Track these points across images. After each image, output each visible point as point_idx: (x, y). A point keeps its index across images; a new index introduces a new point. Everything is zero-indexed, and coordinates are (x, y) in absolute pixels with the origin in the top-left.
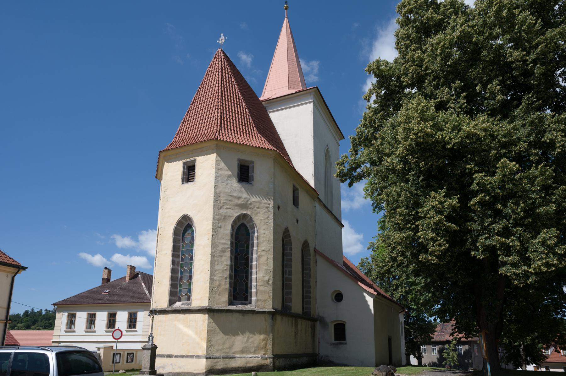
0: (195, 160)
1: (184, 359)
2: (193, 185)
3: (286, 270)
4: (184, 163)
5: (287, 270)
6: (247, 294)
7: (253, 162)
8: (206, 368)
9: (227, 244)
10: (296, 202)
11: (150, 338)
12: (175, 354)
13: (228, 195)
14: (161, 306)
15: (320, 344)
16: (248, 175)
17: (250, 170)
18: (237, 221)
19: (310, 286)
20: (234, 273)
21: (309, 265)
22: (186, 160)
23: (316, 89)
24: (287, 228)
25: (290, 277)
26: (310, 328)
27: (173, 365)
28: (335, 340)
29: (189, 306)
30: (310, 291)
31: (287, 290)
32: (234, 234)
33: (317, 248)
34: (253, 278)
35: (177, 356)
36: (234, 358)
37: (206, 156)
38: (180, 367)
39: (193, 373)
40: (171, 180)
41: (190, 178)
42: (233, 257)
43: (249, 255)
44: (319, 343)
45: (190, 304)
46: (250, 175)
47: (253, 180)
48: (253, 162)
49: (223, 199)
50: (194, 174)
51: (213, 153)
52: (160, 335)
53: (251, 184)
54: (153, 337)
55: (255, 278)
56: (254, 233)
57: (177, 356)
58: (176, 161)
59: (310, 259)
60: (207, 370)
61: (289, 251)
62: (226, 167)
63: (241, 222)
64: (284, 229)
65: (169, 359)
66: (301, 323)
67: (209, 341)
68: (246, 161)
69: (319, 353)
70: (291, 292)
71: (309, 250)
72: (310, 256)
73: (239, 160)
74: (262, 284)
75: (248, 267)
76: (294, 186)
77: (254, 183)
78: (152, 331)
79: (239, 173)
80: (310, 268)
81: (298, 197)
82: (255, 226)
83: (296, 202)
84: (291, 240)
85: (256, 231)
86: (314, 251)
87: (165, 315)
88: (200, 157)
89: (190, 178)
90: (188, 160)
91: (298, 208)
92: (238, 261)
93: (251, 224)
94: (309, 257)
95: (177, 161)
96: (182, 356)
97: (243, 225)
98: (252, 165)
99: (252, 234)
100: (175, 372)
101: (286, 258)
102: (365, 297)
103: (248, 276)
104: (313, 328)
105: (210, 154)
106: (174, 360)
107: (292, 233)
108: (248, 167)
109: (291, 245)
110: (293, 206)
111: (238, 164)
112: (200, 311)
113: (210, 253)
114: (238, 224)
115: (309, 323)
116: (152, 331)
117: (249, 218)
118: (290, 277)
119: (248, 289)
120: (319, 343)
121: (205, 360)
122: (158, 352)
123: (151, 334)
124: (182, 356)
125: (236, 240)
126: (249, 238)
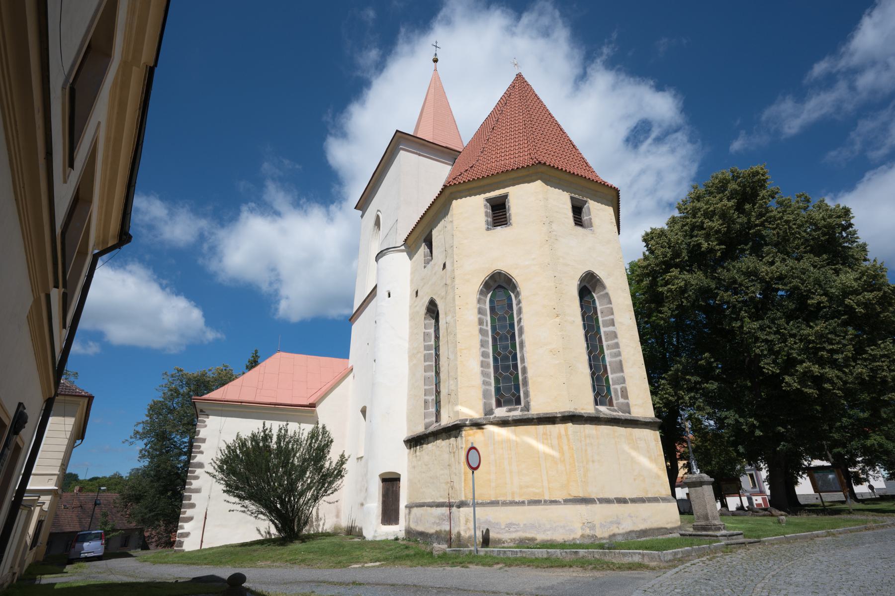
0: (586, 202)
1: (647, 505)
14: (583, 409)
27: (631, 517)
29: (526, 413)
35: (634, 501)
37: (600, 204)
38: (644, 520)
39: (666, 528)
40: (557, 212)
52: (593, 461)
57: (634, 501)
65: (604, 505)
87: (594, 426)
96: (642, 500)
100: (638, 529)
106: (630, 507)
124: (642, 500)
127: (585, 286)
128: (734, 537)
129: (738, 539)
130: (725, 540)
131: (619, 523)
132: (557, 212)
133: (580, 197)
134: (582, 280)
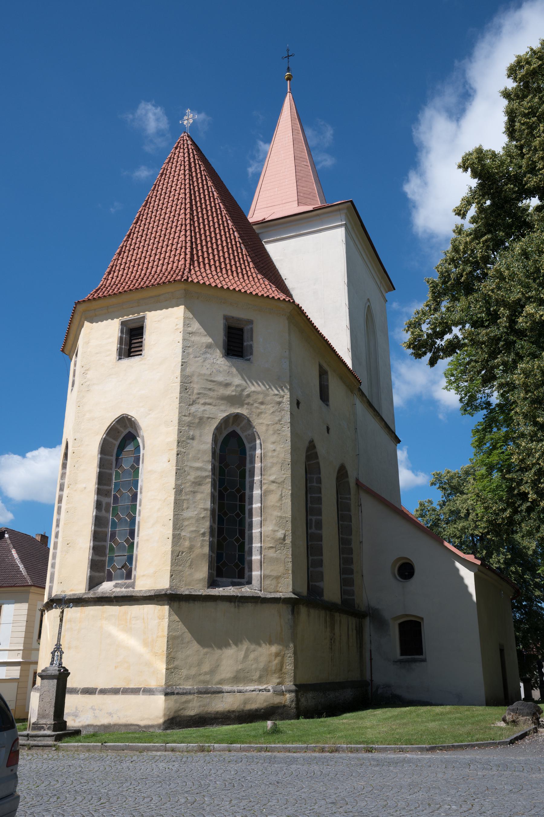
0: (143, 318)
1: (120, 697)
2: (140, 361)
3: (311, 520)
4: (123, 324)
5: (314, 518)
6: (243, 564)
7: (251, 322)
8: (165, 715)
9: (206, 470)
10: (324, 396)
11: (56, 654)
12: (100, 686)
13: (207, 380)
15: (373, 661)
16: (242, 344)
17: (246, 336)
18: (223, 427)
19: (351, 549)
20: (218, 524)
21: (349, 510)
22: (126, 318)
23: (350, 203)
24: (313, 441)
25: (319, 532)
26: (355, 632)
27: (94, 710)
28: (402, 654)
30: (352, 558)
31: (315, 558)
32: (218, 451)
33: (360, 480)
34: (254, 535)
35: (103, 692)
36: (221, 692)
37: (164, 310)
38: (110, 714)
39: (138, 725)
40: (97, 353)
41: (133, 350)
42: (217, 494)
43: (244, 489)
44: (371, 659)
45: (133, 585)
46: (245, 344)
47: (251, 354)
48: (251, 322)
49: (196, 387)
50: (142, 342)
51: (178, 305)
53: (249, 360)
54: (62, 653)
55: (259, 535)
56: (255, 449)
57: (103, 692)
58: (107, 320)
59: (350, 499)
60: (167, 718)
61: (315, 484)
62: (202, 330)
63: (230, 430)
64: (307, 444)
66: (340, 621)
67: (170, 659)
68: (238, 320)
69: (372, 680)
70: (322, 561)
71: (348, 483)
72: (350, 494)
73: (226, 318)
74: (271, 545)
75: (244, 514)
76: (320, 367)
77: (253, 358)
78: (59, 639)
79: (226, 340)
80: (351, 516)
81: (327, 386)
82: (257, 437)
83: (324, 396)
84: (318, 463)
85: (258, 446)
86: (356, 484)
88: (153, 313)
89: (133, 350)
90: (131, 317)
91: (327, 405)
92: (226, 502)
93: (250, 432)
94: (348, 496)
95: (110, 320)
96: (115, 691)
97: (234, 435)
98: (249, 327)
99: (250, 451)
100: (99, 723)
101: (310, 497)
102: (457, 570)
103: (244, 530)
104: (360, 631)
105: (173, 307)
106: (97, 699)
107: (321, 450)
108: (241, 330)
109: (320, 473)
110: (321, 402)
111: (225, 325)
112: (154, 599)
113: (173, 486)
114: (225, 433)
115: (353, 621)
116: (59, 639)
117: (245, 421)
118: (319, 532)
119: (244, 555)
120: (371, 659)
121: (162, 697)
122: (71, 683)
123: (56, 645)
124: (115, 691)
125: (220, 463)
126: (245, 458)
127: (130, 432)
128: (39, 738)
129: (44, 740)
130: (24, 740)
131: (76, 716)
132: (97, 353)
133: (136, 316)
134: (112, 431)
